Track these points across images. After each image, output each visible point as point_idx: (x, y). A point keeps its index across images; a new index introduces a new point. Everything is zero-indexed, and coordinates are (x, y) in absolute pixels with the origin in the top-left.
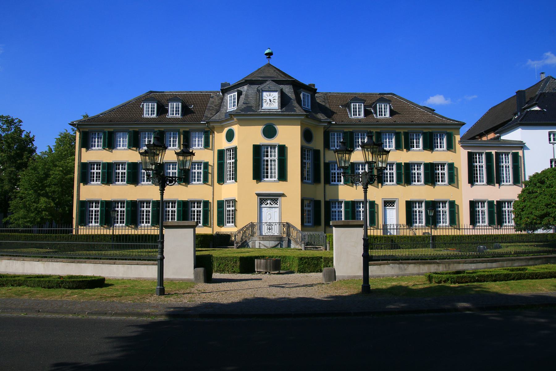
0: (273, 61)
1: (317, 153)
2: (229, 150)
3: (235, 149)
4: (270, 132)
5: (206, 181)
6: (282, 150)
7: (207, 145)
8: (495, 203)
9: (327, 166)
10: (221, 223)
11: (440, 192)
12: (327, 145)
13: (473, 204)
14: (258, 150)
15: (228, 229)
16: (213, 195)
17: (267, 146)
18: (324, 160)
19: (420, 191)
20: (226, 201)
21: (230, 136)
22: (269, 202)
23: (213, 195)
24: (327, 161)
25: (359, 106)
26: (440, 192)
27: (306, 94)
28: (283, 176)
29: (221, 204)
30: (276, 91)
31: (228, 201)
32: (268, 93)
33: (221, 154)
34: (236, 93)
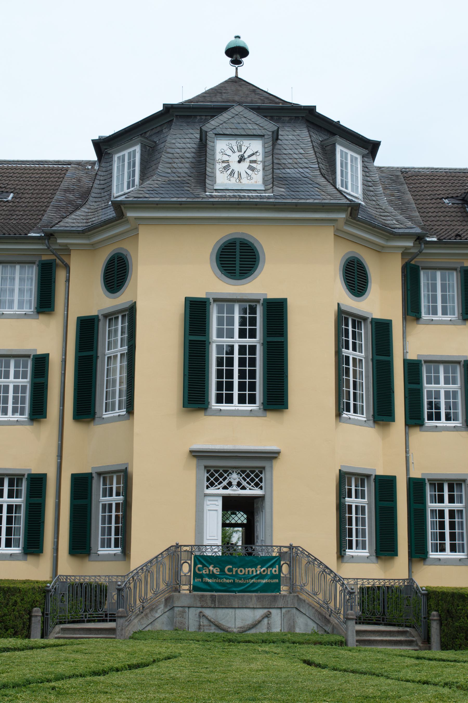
0: (249, 71)
1: (382, 330)
2: (111, 317)
3: (130, 312)
4: (238, 259)
5: (38, 411)
6: (277, 311)
7: (45, 303)
9: (413, 369)
10: (80, 545)
12: (412, 309)
14: (196, 313)
15: (100, 568)
16: (60, 456)
17: (226, 302)
18: (405, 353)
20: (99, 474)
21: (117, 274)
22: (235, 478)
23: (60, 456)
24: (412, 356)
27: (350, 153)
29: (82, 484)
30: (261, 136)
31: (105, 475)
33: (88, 330)
34: (137, 148)
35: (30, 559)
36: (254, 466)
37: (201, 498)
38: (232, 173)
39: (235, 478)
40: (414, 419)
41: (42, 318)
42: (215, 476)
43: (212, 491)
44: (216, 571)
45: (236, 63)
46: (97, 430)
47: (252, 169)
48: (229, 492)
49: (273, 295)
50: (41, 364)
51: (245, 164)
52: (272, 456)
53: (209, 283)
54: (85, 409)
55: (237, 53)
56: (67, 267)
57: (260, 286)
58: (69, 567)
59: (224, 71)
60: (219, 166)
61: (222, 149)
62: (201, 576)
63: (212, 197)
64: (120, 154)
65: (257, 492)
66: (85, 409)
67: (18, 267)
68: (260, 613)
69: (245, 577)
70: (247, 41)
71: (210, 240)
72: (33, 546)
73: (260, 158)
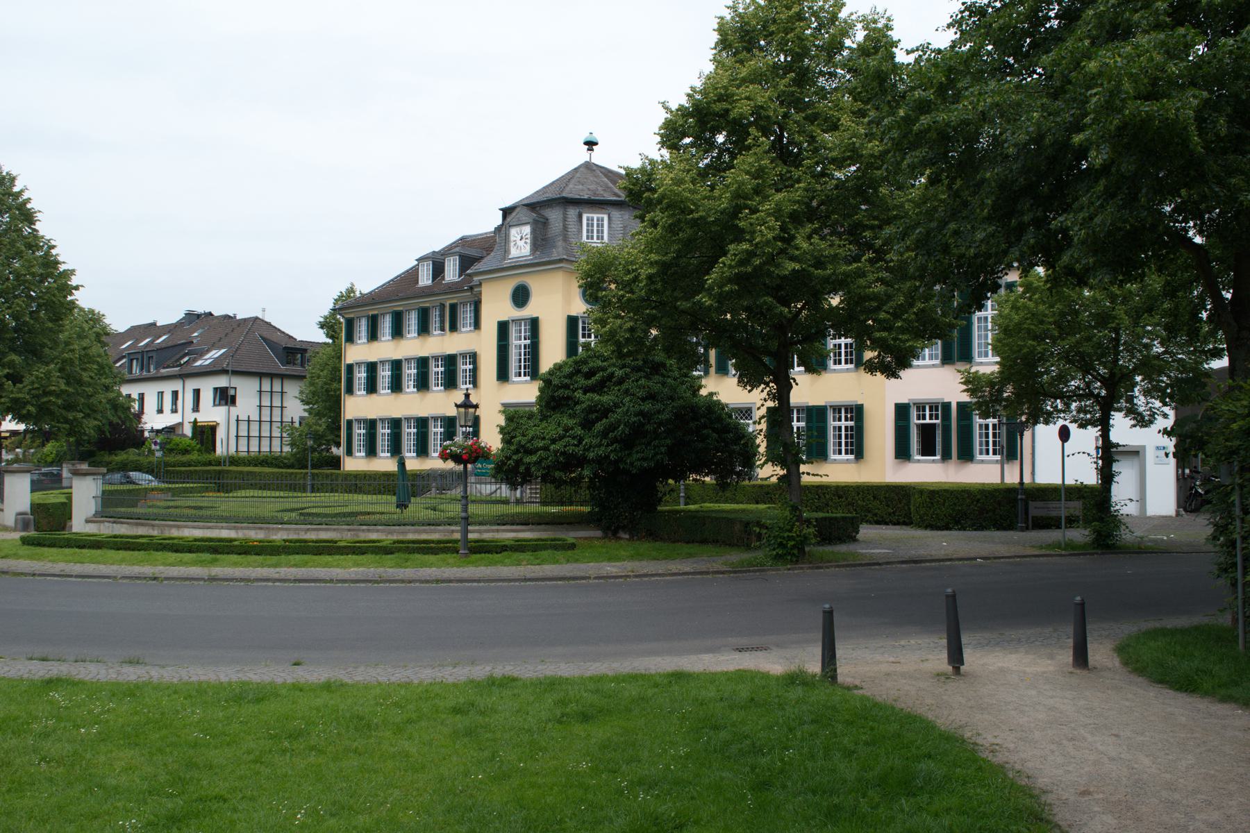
4: (521, 296)
6: (534, 324)
8: (954, 406)
13: (902, 411)
17: (517, 321)
32: (518, 229)
45: (591, 149)
53: (508, 311)
55: (591, 144)
57: (528, 312)
68: (494, 487)
70: (597, 137)
71: (507, 288)
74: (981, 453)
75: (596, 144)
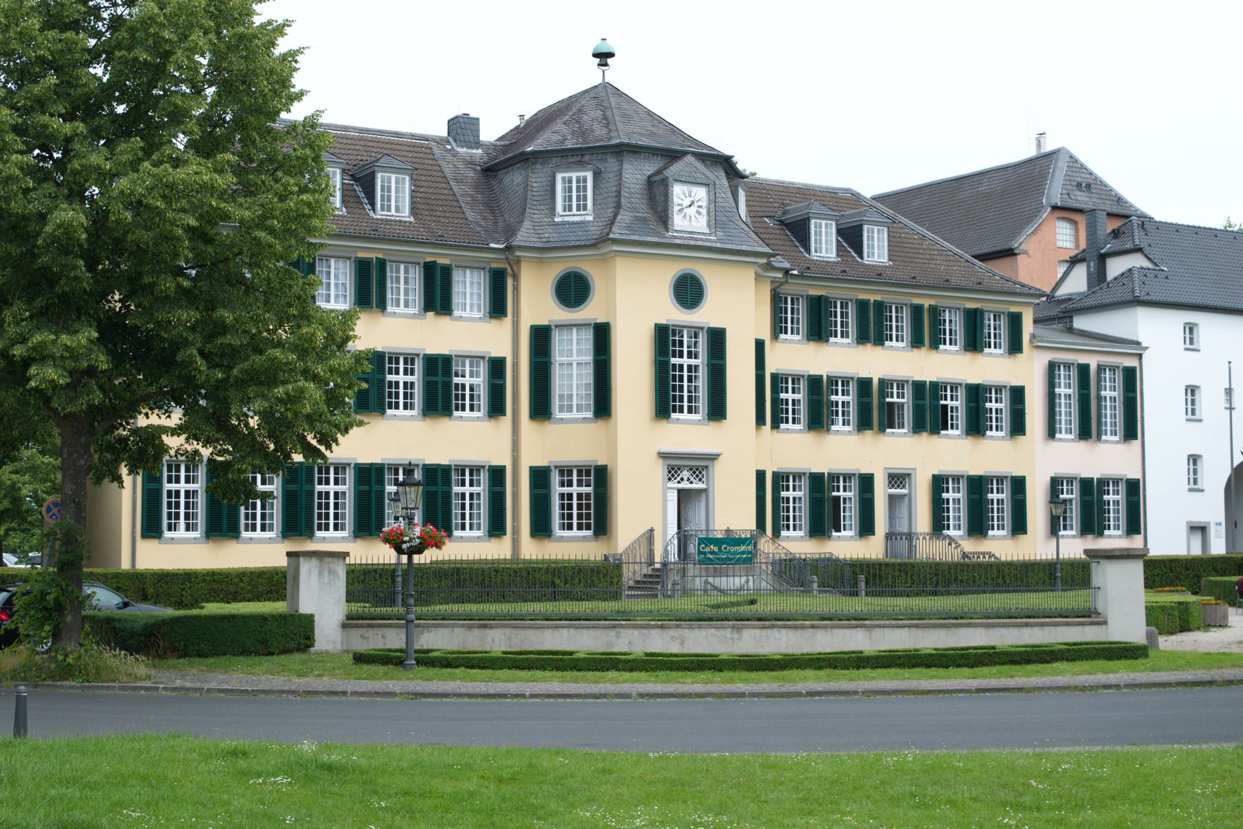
4: (689, 291)
6: (717, 339)
7: (497, 308)
10: (541, 528)
11: (990, 455)
19: (954, 453)
21: (573, 290)
22: (686, 474)
25: (397, 182)
26: (990, 455)
28: (717, 411)
29: (540, 477)
33: (541, 338)
35: (494, 540)
36: (701, 464)
37: (665, 489)
38: (685, 216)
39: (686, 474)
40: (775, 425)
41: (494, 322)
42: (673, 472)
43: (670, 484)
44: (716, 549)
46: (549, 428)
47: (699, 213)
48: (681, 486)
49: (715, 324)
50: (497, 367)
51: (694, 208)
52: (713, 458)
54: (541, 408)
55: (603, 57)
56: (516, 277)
57: (706, 315)
58: (531, 550)
59: (590, 76)
60: (676, 208)
61: (680, 193)
62: (705, 553)
63: (675, 237)
64: (567, 175)
65: (701, 486)
66: (541, 408)
67: (468, 271)
69: (735, 553)
72: (497, 527)
73: (704, 204)
74: (247, 530)
75: (611, 55)
